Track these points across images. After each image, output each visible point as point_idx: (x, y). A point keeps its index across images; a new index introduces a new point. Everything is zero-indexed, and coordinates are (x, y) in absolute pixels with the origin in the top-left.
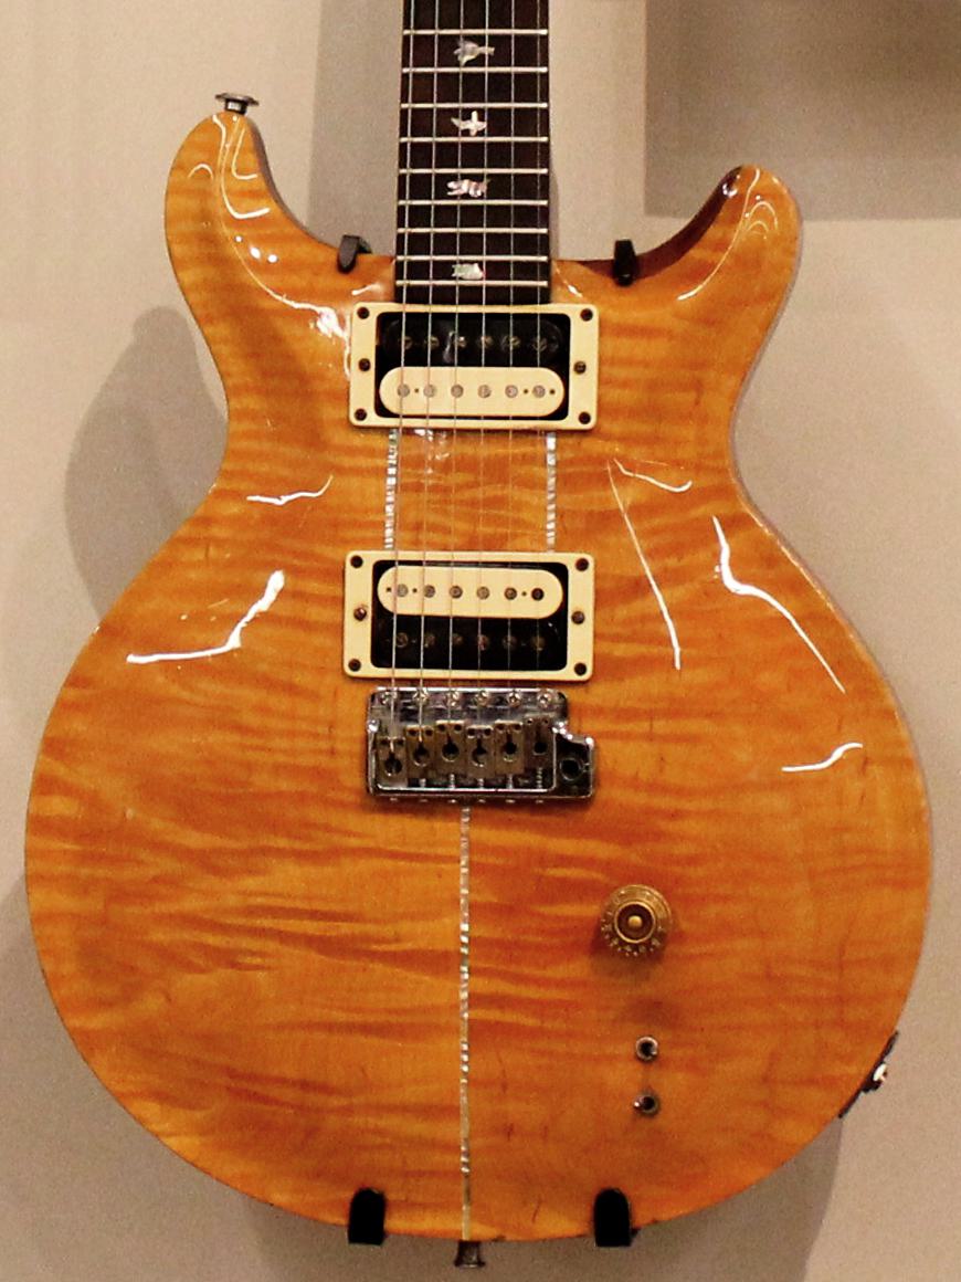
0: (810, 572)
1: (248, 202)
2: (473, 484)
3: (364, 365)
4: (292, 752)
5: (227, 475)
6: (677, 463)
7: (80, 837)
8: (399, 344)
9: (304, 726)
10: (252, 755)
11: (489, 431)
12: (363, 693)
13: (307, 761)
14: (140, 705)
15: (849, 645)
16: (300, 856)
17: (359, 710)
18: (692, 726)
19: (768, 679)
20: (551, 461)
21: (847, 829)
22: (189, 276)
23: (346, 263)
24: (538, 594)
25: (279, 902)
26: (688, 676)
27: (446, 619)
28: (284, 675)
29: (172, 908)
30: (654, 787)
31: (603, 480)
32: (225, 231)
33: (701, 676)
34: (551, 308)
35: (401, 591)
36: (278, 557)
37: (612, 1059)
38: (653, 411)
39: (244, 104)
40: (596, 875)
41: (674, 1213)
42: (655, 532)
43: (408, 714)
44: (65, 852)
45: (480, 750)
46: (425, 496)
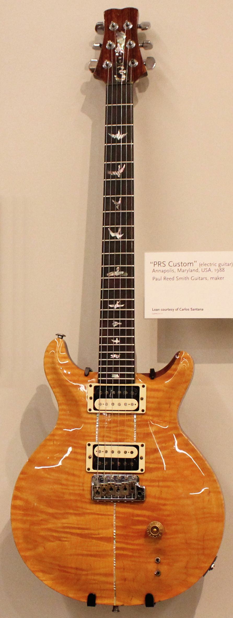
0: (196, 447)
1: (63, 360)
2: (116, 427)
3: (91, 398)
4: (74, 490)
5: (58, 424)
6: (165, 421)
7: (24, 510)
8: (99, 393)
9: (77, 484)
10: (64, 491)
11: (120, 414)
12: (90, 476)
13: (77, 492)
14: (38, 479)
15: (206, 464)
16: (75, 514)
17: (90, 480)
18: (169, 484)
19: (187, 473)
20: (135, 421)
21: (205, 508)
22: (49, 377)
23: (86, 374)
24: (132, 452)
25: (71, 525)
26: (167, 472)
27: (110, 458)
28: (72, 471)
29: (45, 527)
30: (159, 498)
31: (147, 425)
32: (58, 366)
33: (170, 472)
34: (135, 385)
35: (100, 452)
36: (70, 444)
37: (149, 563)
38: (159, 409)
39: (63, 336)
40: (146, 519)
41: (164, 599)
42: (160, 438)
43: (101, 481)
44: (20, 513)
45: (118, 489)
46: (105, 429)
